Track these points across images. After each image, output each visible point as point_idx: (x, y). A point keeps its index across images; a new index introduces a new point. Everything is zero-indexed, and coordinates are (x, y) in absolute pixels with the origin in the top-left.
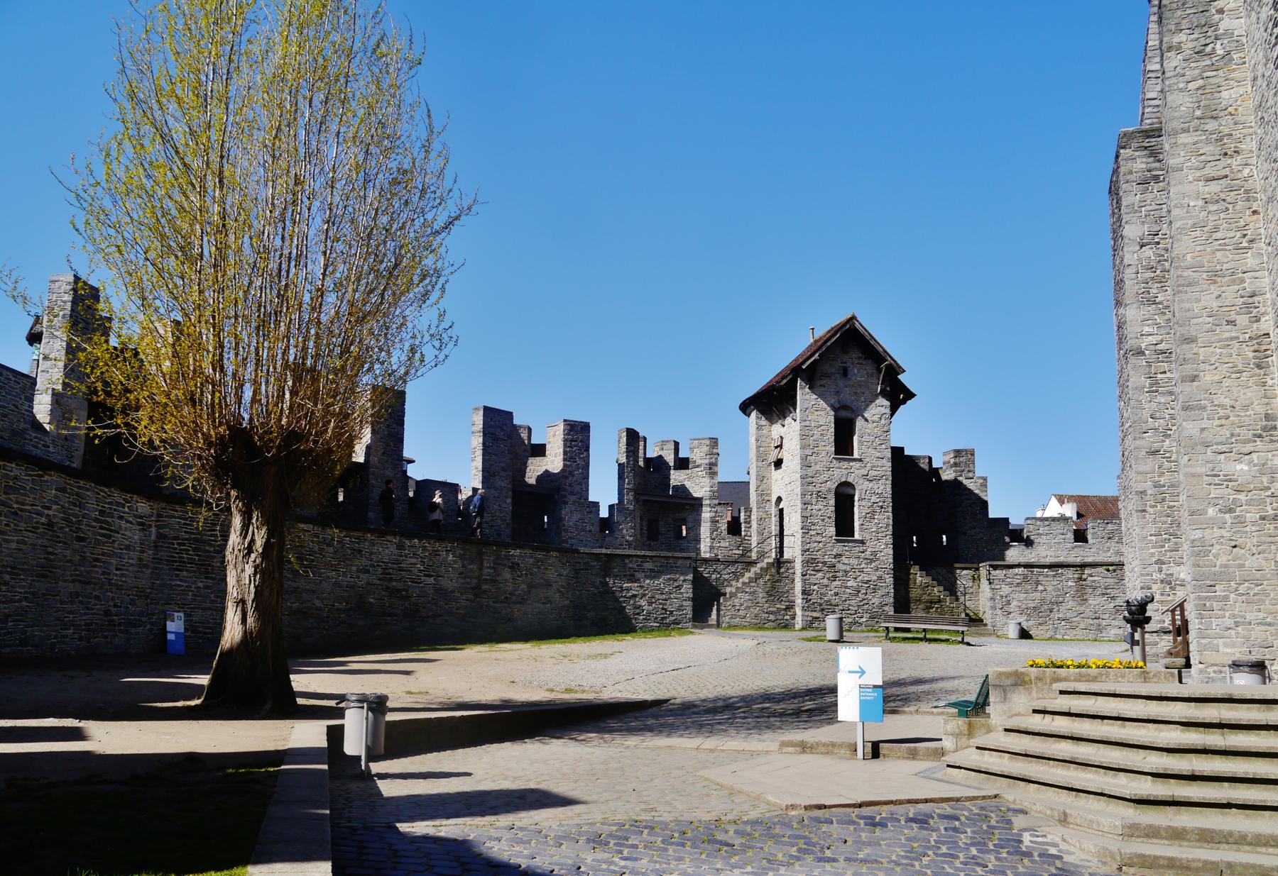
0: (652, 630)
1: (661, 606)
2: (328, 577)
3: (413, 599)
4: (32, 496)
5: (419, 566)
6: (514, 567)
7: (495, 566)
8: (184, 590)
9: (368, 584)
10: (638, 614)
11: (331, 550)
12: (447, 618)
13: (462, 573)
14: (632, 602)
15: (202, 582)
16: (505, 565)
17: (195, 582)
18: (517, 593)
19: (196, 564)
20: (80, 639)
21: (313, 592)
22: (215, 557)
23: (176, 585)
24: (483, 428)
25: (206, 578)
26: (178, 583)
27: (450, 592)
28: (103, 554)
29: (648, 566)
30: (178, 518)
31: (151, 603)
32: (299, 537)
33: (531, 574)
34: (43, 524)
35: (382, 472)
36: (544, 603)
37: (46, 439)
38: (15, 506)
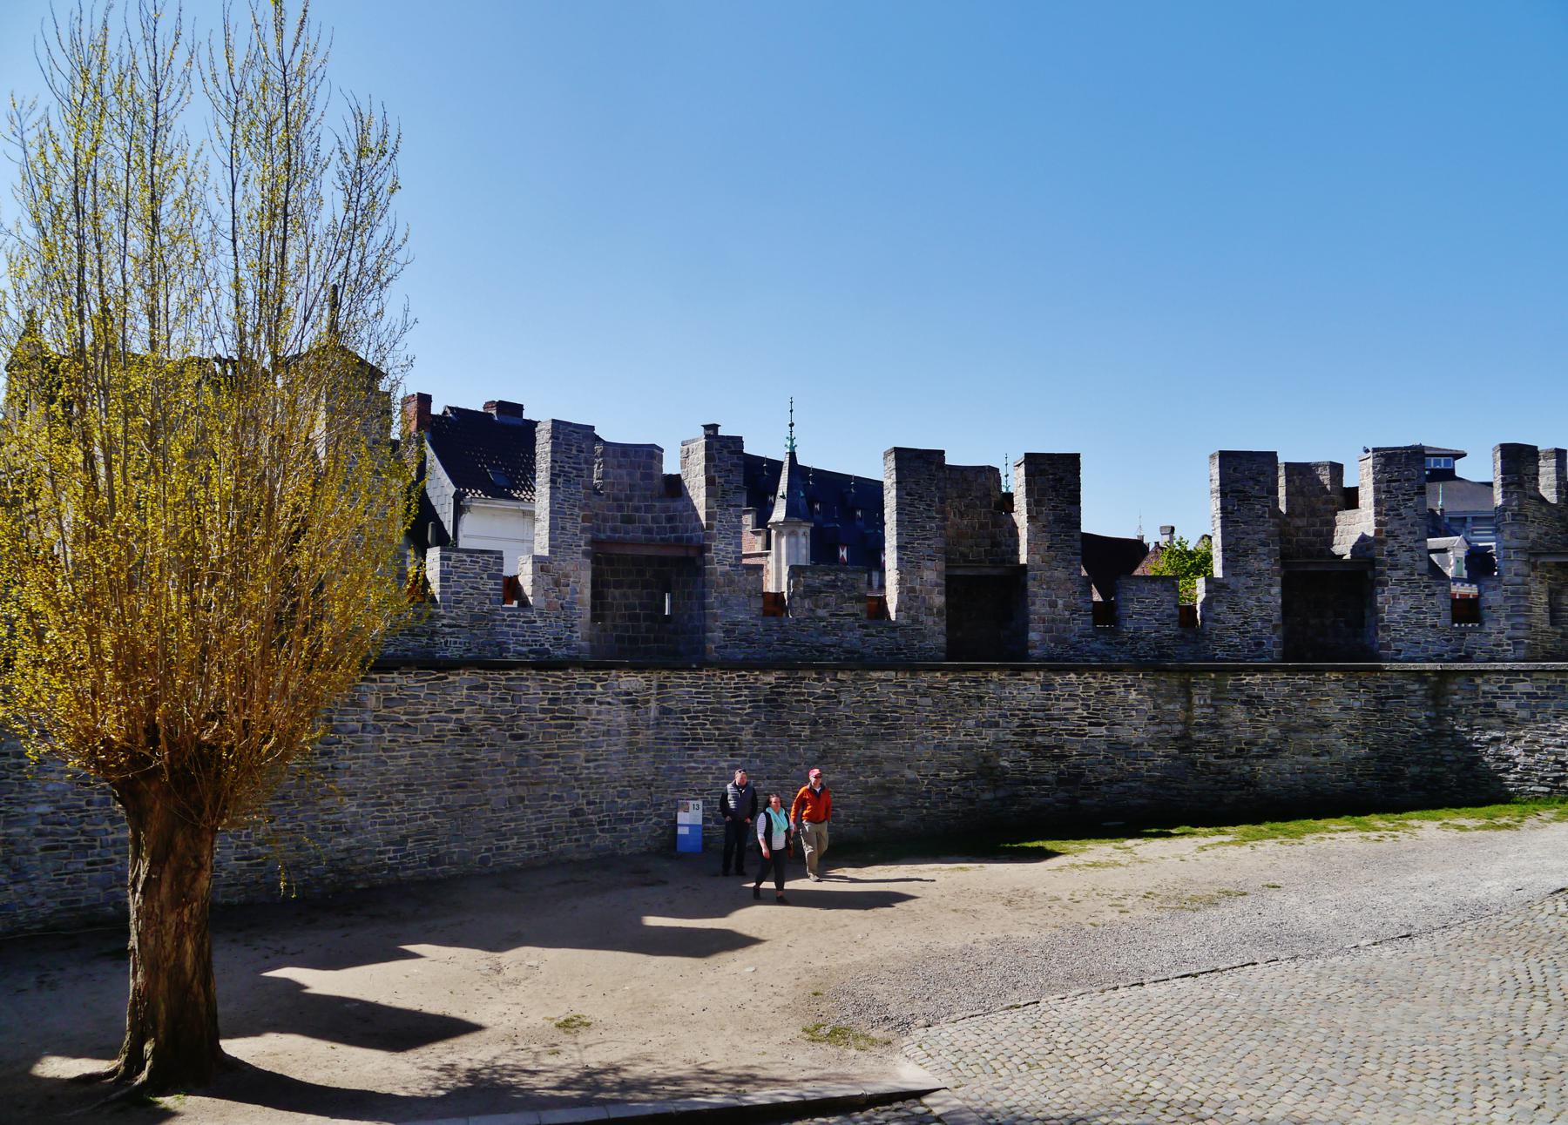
0: (1536, 798)
1: (1553, 758)
2: (926, 738)
3: (1073, 760)
4: (429, 702)
5: (1079, 711)
6: (1252, 702)
7: (1216, 703)
8: (702, 773)
9: (997, 741)
10: (1506, 771)
11: (928, 701)
12: (1132, 784)
13: (1154, 718)
14: (1491, 750)
15: (726, 761)
16: (1235, 701)
17: (716, 762)
18: (1260, 742)
19: (716, 740)
20: (531, 847)
21: (901, 759)
22: (743, 729)
23: (689, 768)
24: (1221, 485)
25: (732, 756)
26: (693, 765)
27: (1135, 746)
28: (560, 748)
29: (1519, 687)
30: (687, 686)
31: (656, 792)
32: (874, 690)
33: (1286, 710)
34: (450, 730)
35: (1048, 574)
36: (1314, 755)
37: (529, 614)
38: (404, 718)
